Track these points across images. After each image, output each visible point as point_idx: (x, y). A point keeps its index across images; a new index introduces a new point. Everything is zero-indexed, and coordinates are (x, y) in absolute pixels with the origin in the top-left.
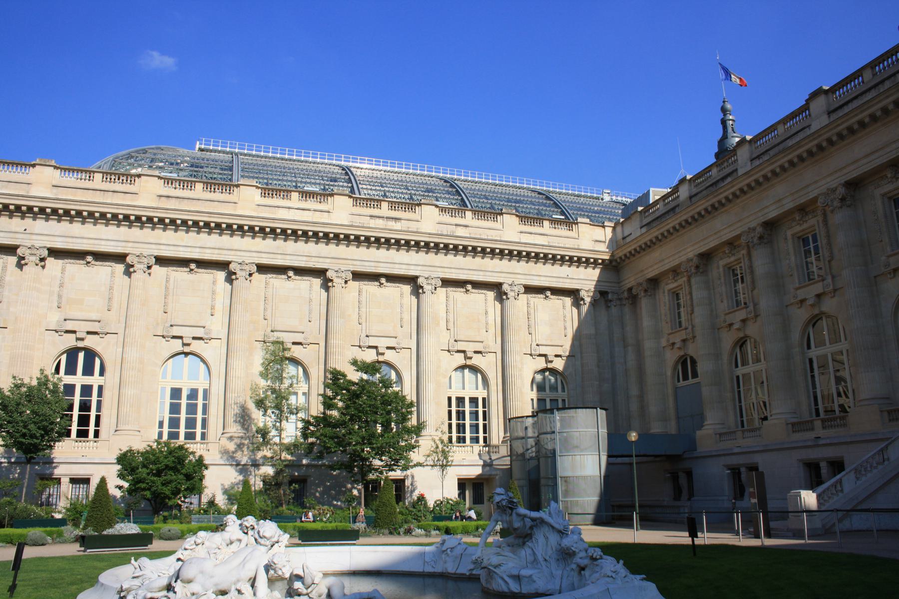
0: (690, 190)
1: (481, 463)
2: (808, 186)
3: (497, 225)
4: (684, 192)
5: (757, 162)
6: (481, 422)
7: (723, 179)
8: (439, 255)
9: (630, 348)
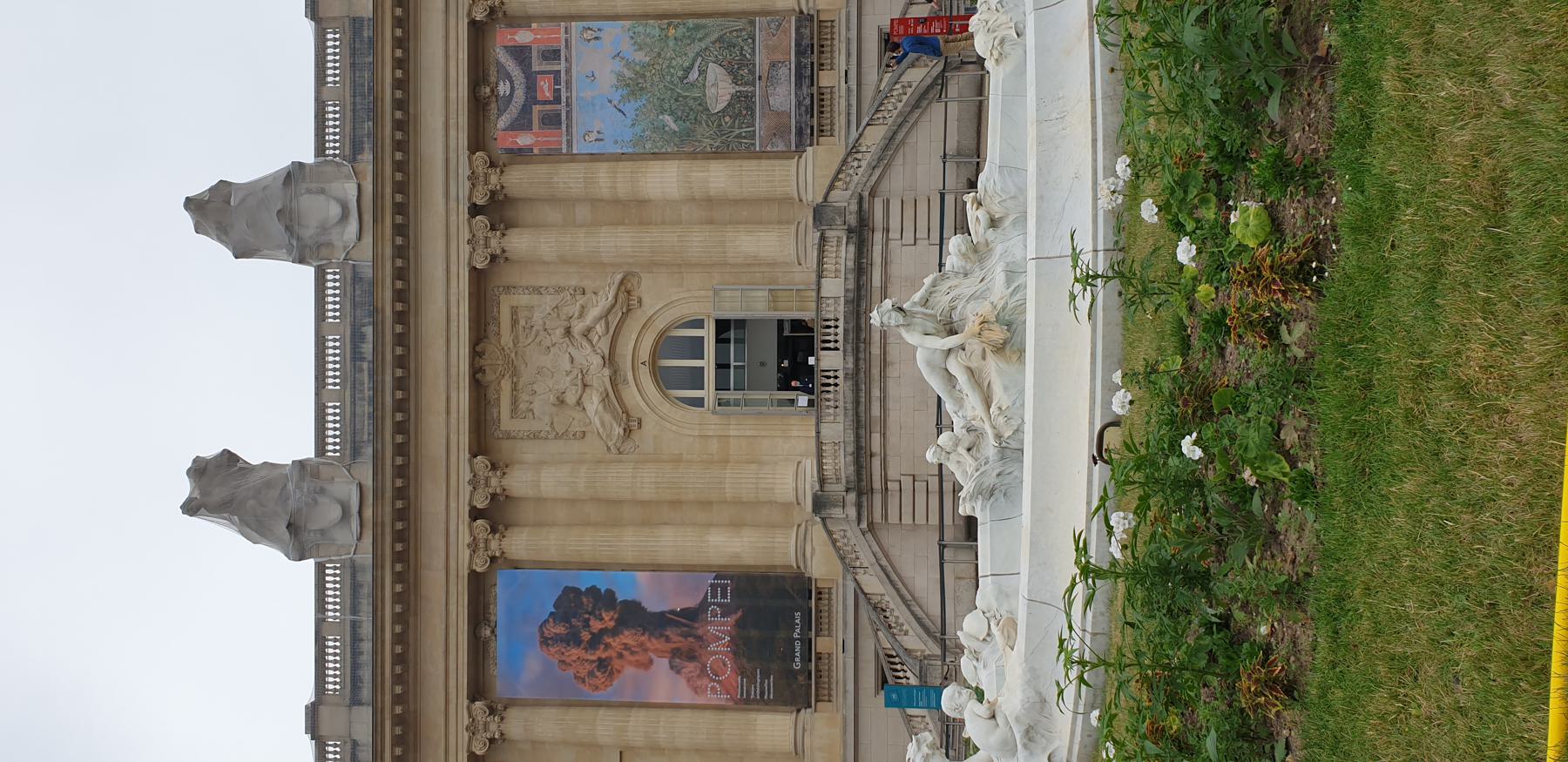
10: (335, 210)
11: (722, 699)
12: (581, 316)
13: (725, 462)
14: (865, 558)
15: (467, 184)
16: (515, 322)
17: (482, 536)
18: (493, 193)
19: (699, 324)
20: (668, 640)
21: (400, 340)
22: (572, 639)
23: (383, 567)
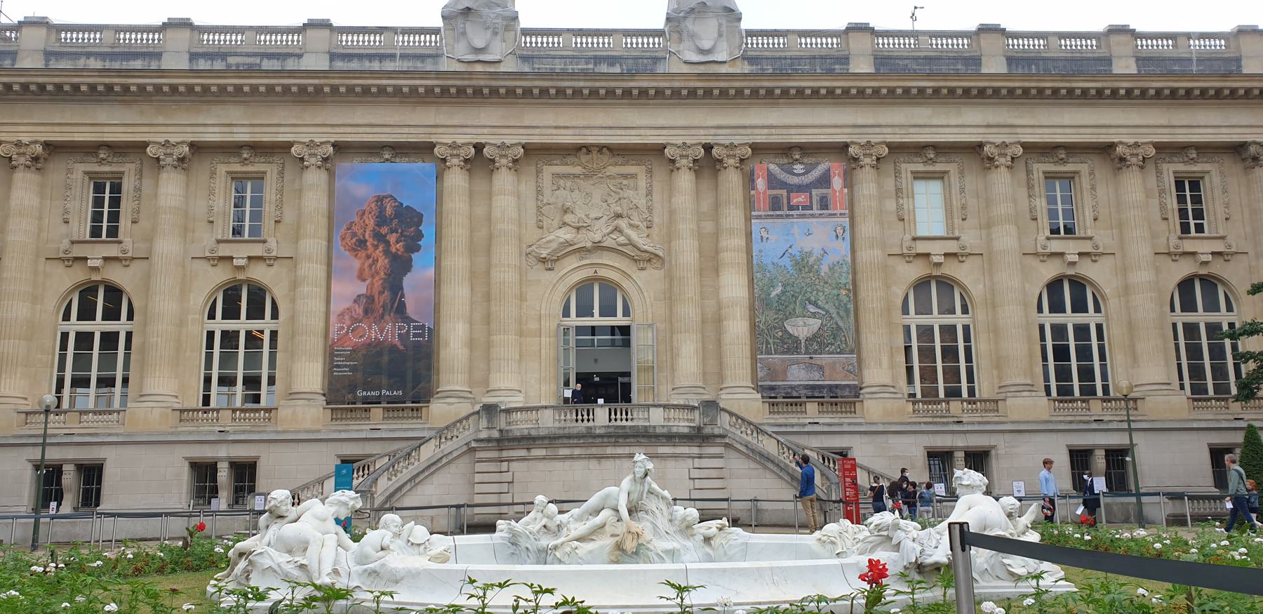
10: (706, 45)
11: (334, 335)
12: (631, 225)
13: (521, 334)
14: (448, 446)
15: (727, 142)
16: (625, 176)
17: (462, 152)
18: (721, 161)
19: (626, 313)
20: (381, 293)
21: (611, 93)
22: (381, 220)
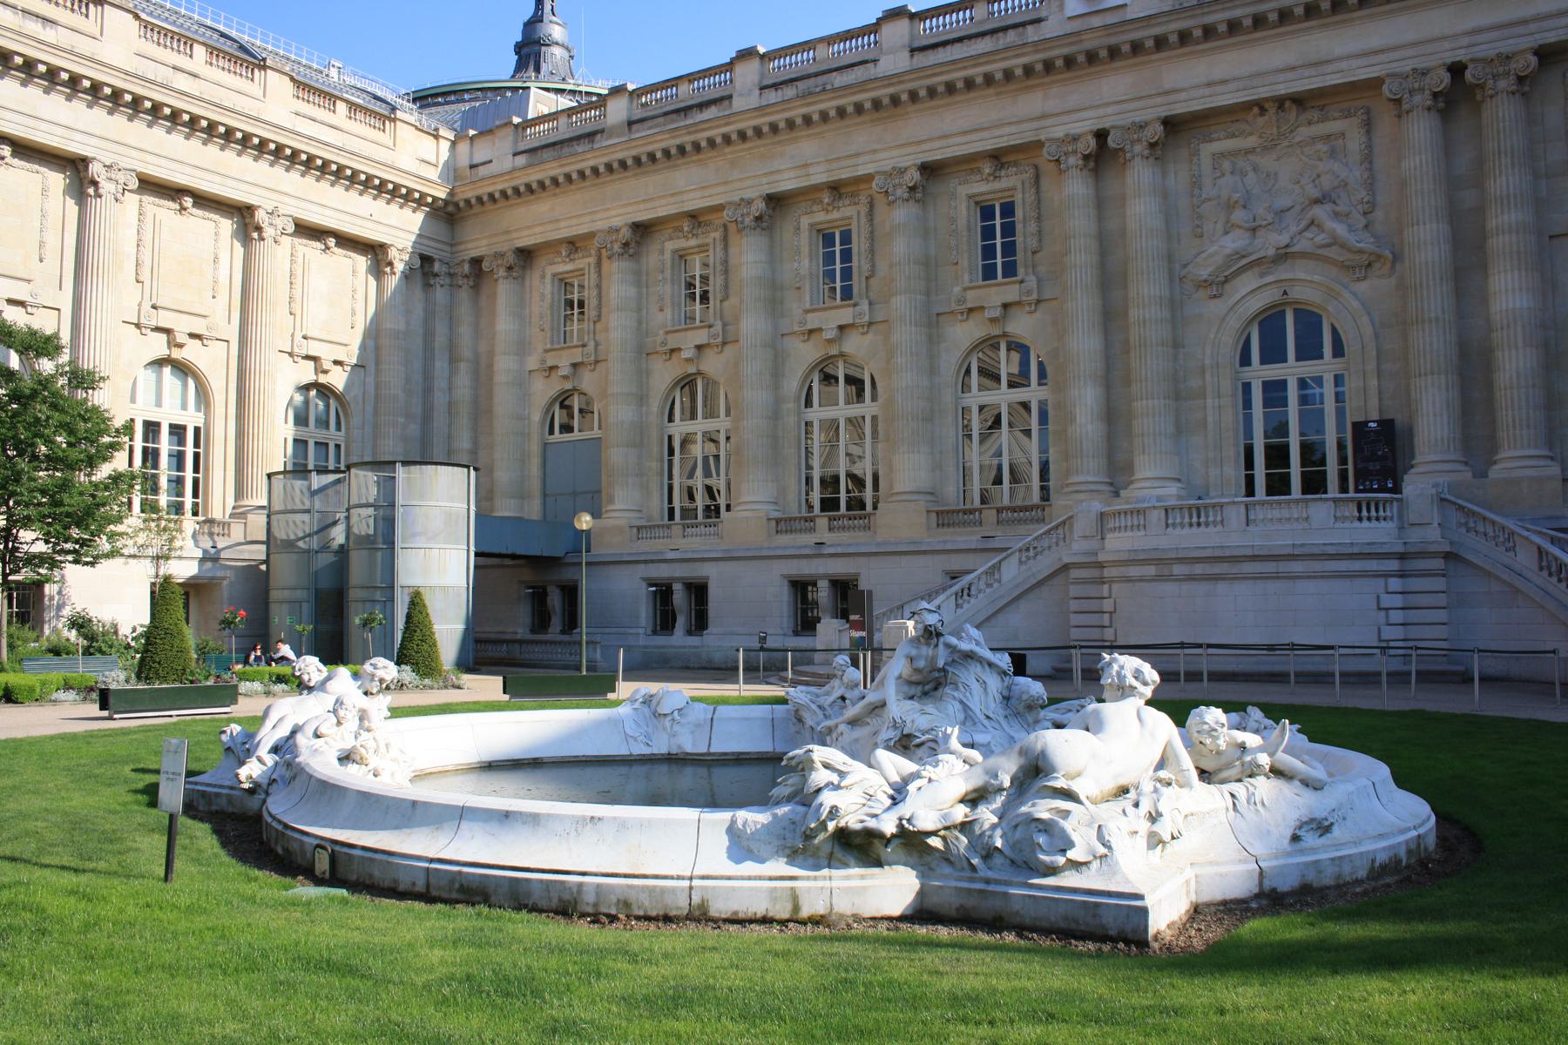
0: (630, 109)
1: (200, 554)
2: (858, 155)
3: (254, 89)
4: (617, 111)
5: (772, 96)
6: (189, 474)
7: (702, 106)
8: (136, 123)
9: (463, 366)
23: (1037, 51)
